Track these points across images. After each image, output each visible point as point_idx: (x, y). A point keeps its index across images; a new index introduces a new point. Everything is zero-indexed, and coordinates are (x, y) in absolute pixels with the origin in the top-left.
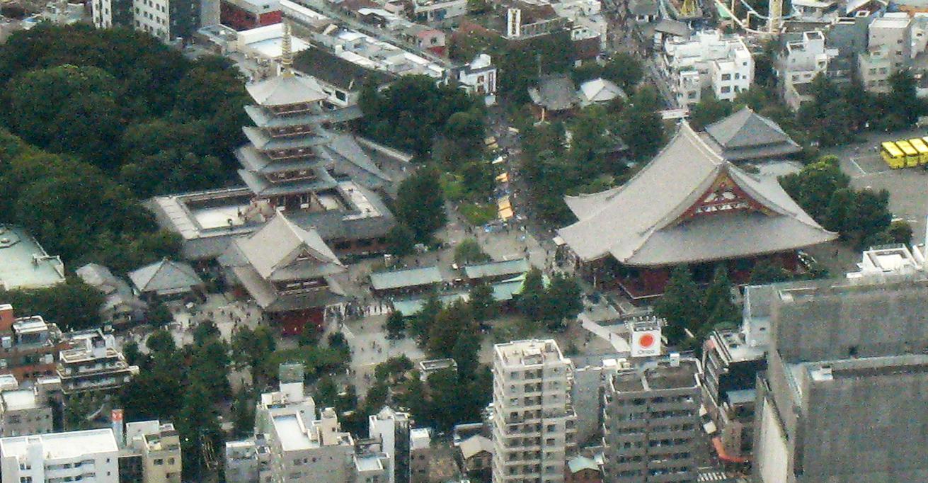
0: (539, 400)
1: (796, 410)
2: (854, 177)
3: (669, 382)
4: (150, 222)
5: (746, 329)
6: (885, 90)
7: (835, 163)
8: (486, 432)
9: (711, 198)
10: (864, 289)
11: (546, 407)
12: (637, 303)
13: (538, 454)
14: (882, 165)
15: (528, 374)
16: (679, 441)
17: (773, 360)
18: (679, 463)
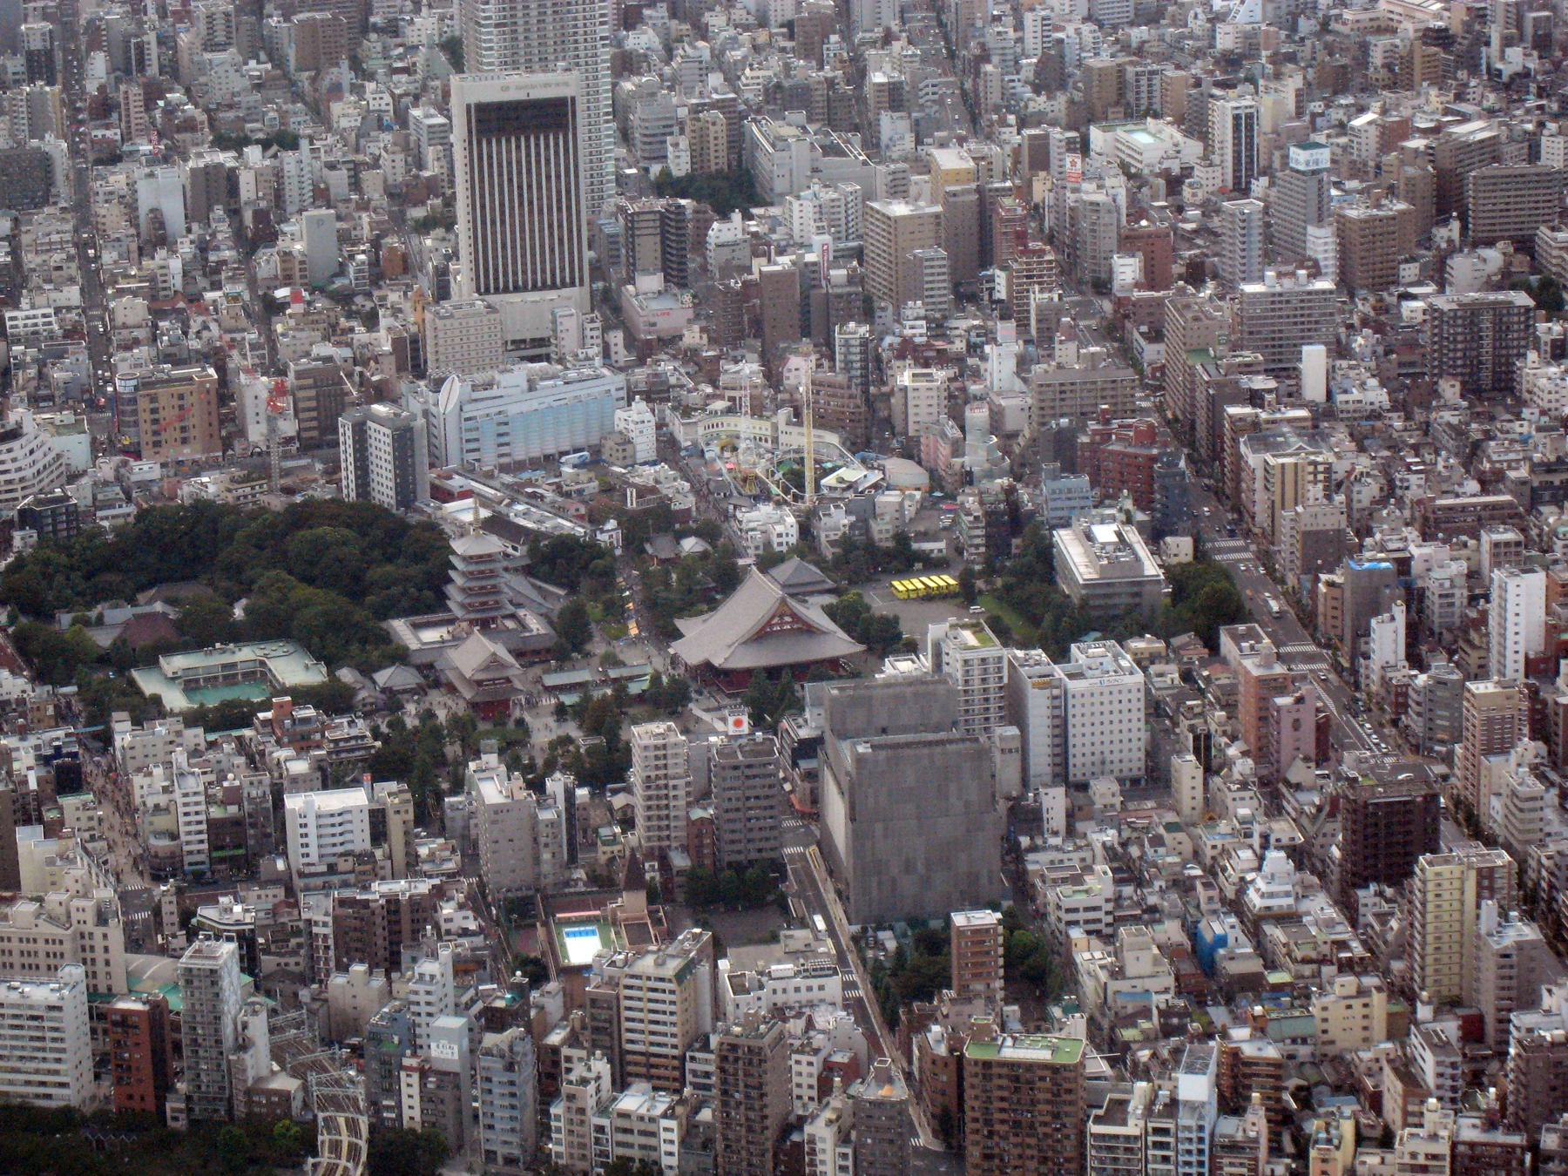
0: (665, 766)
1: (848, 774)
2: (874, 605)
3: (757, 754)
4: (386, 638)
5: (807, 715)
6: (890, 544)
7: (860, 595)
8: (628, 790)
9: (776, 620)
10: (888, 685)
11: (670, 772)
12: (729, 696)
13: (667, 806)
14: (892, 595)
15: (657, 748)
16: (767, 797)
17: (828, 737)
18: (768, 813)
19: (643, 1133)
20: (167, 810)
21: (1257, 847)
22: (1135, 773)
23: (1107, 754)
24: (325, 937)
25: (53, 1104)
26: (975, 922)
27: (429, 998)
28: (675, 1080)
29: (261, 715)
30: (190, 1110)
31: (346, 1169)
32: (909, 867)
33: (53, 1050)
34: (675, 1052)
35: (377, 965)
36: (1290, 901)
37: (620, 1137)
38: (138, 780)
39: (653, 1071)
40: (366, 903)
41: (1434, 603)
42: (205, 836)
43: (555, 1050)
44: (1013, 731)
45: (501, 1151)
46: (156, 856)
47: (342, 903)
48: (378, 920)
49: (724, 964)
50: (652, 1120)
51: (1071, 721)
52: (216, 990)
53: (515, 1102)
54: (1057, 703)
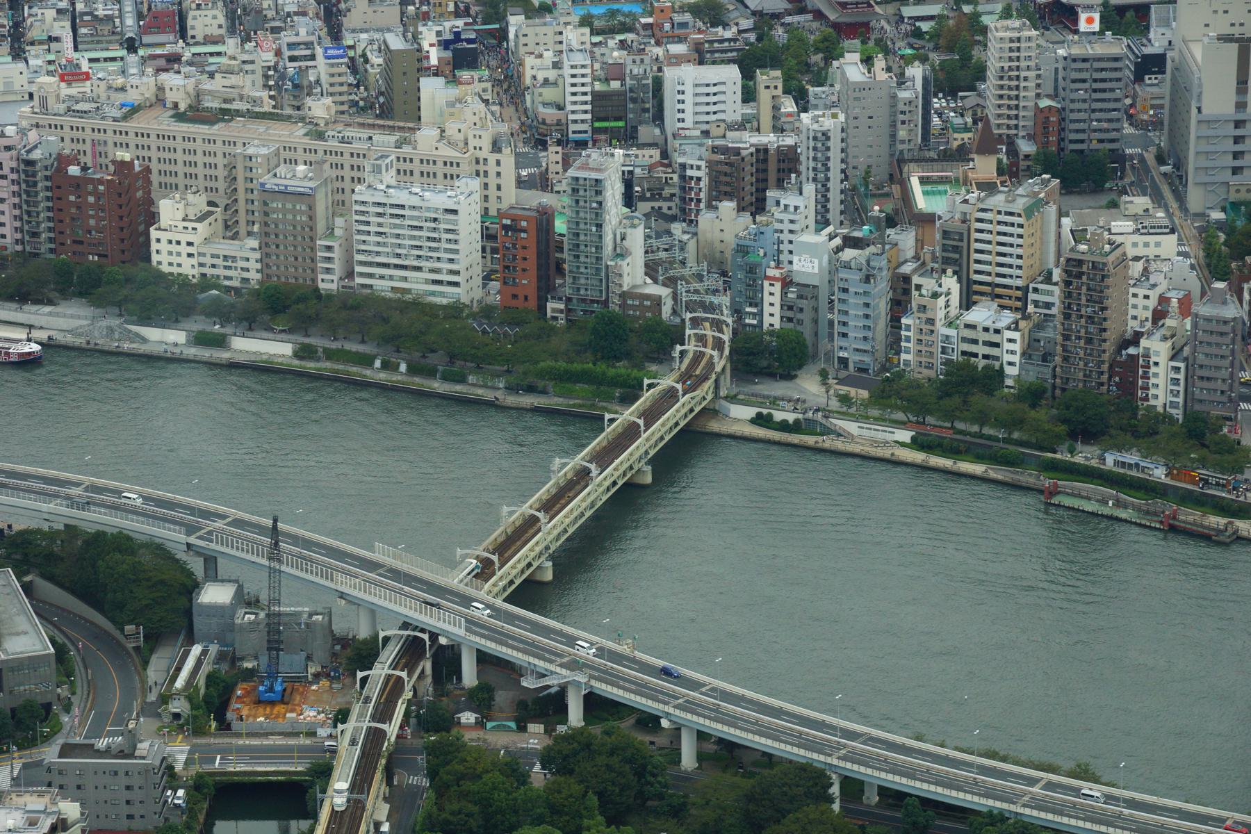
13: (1017, 88)
15: (1011, 40)
19: (986, 343)
20: (555, 84)
24: (699, 179)
25: (445, 301)
27: (792, 227)
28: (1018, 299)
30: (569, 311)
31: (712, 356)
33: (446, 250)
34: (1019, 283)
35: (743, 209)
38: (530, 61)
42: (589, 107)
43: (906, 279)
46: (544, 122)
47: (715, 150)
49: (1066, 221)
50: (997, 331)
52: (599, 198)
53: (868, 311)
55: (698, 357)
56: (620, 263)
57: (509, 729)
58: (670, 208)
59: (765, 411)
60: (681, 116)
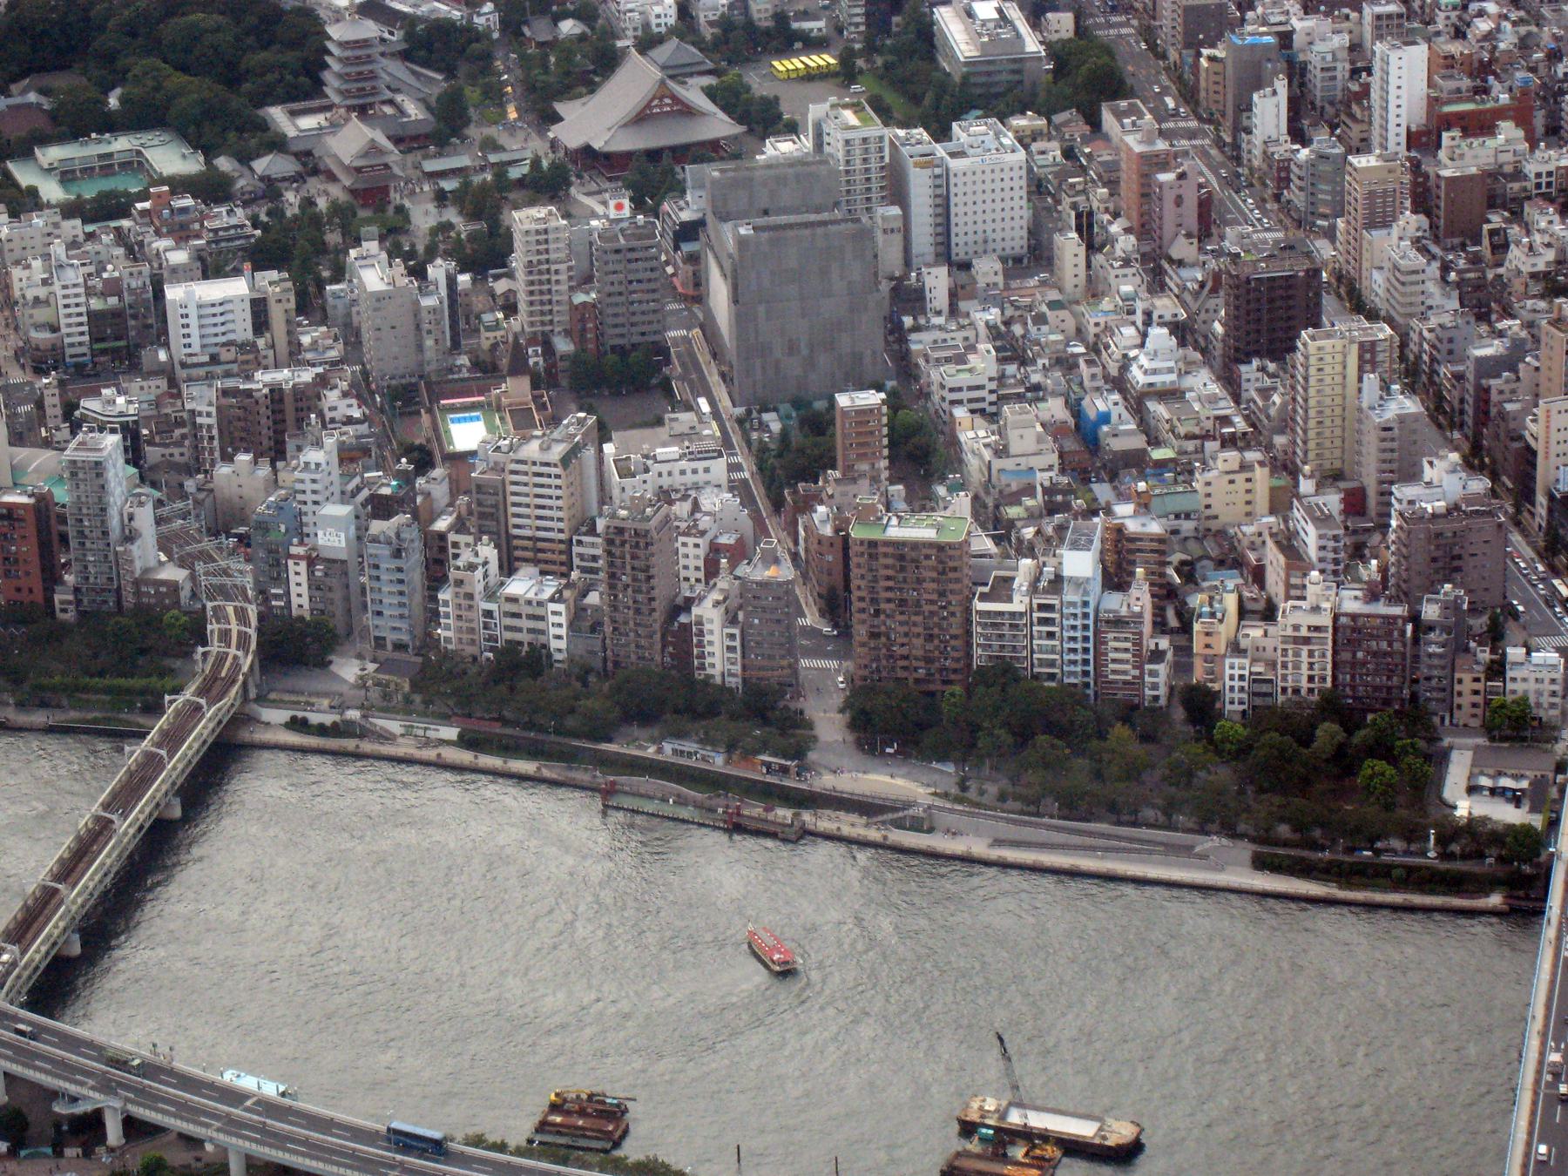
1: (730, 256)
2: (755, 86)
3: (640, 238)
4: (263, 126)
5: (689, 197)
6: (770, 24)
7: (740, 76)
8: (510, 275)
9: (656, 102)
10: (769, 166)
11: (553, 256)
12: (610, 179)
14: (772, 76)
15: (538, 232)
16: (650, 280)
17: (710, 219)
18: (651, 296)
20: (47, 302)
21: (1139, 323)
22: (1018, 251)
23: (989, 232)
24: (210, 427)
26: (859, 402)
28: (562, 564)
29: (139, 206)
30: (78, 602)
31: (235, 657)
32: (792, 349)
34: (562, 536)
35: (262, 455)
36: (1173, 377)
37: (509, 621)
38: (17, 273)
39: (540, 555)
40: (249, 394)
41: (1316, 78)
42: (85, 328)
43: (442, 536)
44: (895, 211)
45: (391, 637)
46: (37, 349)
47: (225, 393)
48: (263, 410)
49: (609, 448)
50: (540, 604)
51: (953, 200)
54: (938, 182)
55: (221, 658)
56: (129, 546)
57: (46, 1156)
58: (182, 454)
59: (300, 714)
60: (187, 341)
